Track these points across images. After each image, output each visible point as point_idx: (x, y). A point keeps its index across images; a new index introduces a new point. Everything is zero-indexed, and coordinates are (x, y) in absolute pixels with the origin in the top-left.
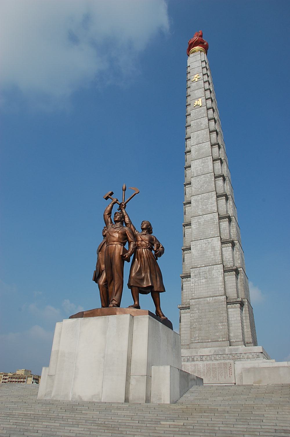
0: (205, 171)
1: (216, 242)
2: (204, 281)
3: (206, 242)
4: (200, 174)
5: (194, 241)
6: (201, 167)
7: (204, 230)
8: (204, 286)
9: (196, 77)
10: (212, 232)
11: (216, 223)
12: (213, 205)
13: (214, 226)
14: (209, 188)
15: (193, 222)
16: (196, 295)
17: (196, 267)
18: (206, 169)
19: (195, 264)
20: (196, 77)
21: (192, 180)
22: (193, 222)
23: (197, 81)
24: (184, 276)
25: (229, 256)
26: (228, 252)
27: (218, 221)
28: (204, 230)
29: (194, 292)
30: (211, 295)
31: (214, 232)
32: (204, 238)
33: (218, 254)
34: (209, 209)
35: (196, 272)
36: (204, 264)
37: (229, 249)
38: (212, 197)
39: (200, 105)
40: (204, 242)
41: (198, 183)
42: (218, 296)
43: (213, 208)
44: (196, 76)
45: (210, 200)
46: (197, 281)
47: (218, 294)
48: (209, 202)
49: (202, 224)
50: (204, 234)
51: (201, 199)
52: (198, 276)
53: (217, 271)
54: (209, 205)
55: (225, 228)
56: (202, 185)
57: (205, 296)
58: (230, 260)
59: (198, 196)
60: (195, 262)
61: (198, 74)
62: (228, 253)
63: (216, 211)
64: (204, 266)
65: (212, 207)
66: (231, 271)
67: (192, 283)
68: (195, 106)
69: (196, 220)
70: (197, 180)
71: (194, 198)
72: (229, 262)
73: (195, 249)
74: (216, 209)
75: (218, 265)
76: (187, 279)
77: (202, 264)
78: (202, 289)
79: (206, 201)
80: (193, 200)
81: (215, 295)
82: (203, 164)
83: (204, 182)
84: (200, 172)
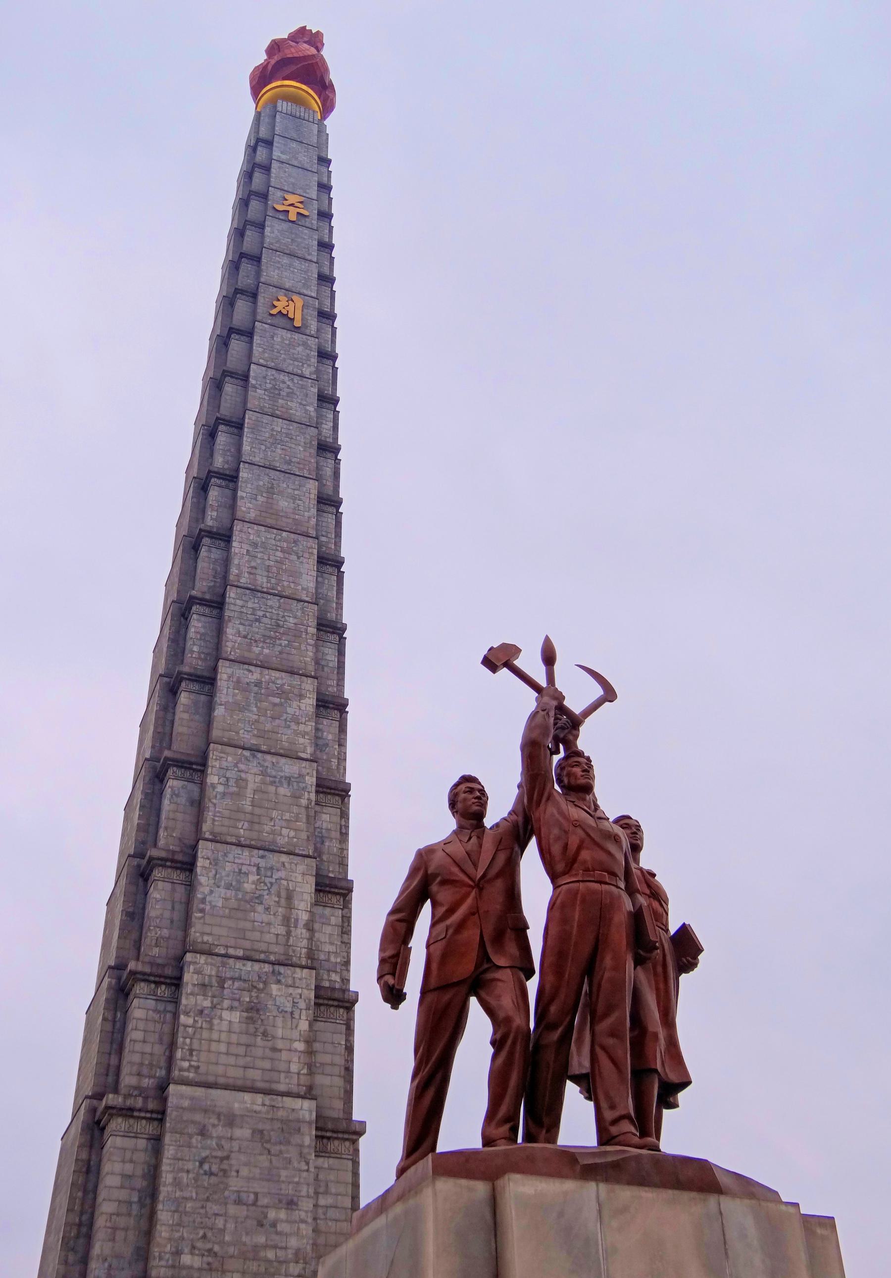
0: (286, 584)
1: (300, 879)
2: (235, 1017)
3: (262, 863)
4: (264, 585)
5: (211, 841)
6: (272, 563)
7: (257, 811)
8: (234, 1038)
9: (292, 205)
10: (285, 831)
11: (304, 802)
12: (302, 727)
13: (295, 809)
14: (291, 657)
15: (217, 764)
16: (198, 1067)
17: (206, 947)
18: (291, 579)
19: (206, 938)
20: (292, 205)
21: (232, 595)
22: (217, 764)
23: (293, 222)
24: (144, 974)
25: (331, 943)
26: (330, 927)
27: (313, 796)
28: (257, 811)
29: (191, 1055)
30: (260, 1085)
31: (292, 834)
32: (253, 843)
33: (301, 924)
34: (284, 738)
35: (208, 970)
36: (244, 949)
37: (333, 918)
38: (301, 696)
39: (298, 324)
40: (253, 859)
41: (251, 617)
42: (288, 1094)
43: (301, 740)
44: (292, 199)
45: (295, 704)
46: (206, 1012)
47: (282, 1088)
48: (289, 710)
49: (251, 786)
50: (256, 827)
51: (258, 684)
52: (215, 989)
53: (291, 990)
54: (286, 720)
55: (328, 830)
56: (267, 633)
57: (231, 1081)
58: (333, 959)
59: (250, 671)
60: (207, 929)
61: (302, 199)
62: (328, 930)
63: (308, 756)
64: (240, 953)
65: (296, 733)
66: (336, 1003)
67: (187, 1014)
68: (274, 311)
69: (230, 759)
70: (250, 605)
71: (229, 671)
72: (326, 965)
73: (211, 875)
74: (309, 750)
75: (298, 970)
76: (153, 986)
77: (232, 942)
78: (223, 1048)
79: (277, 700)
80: (225, 677)
81: (275, 1086)
82: (279, 554)
83: (278, 625)
84: (265, 580)
